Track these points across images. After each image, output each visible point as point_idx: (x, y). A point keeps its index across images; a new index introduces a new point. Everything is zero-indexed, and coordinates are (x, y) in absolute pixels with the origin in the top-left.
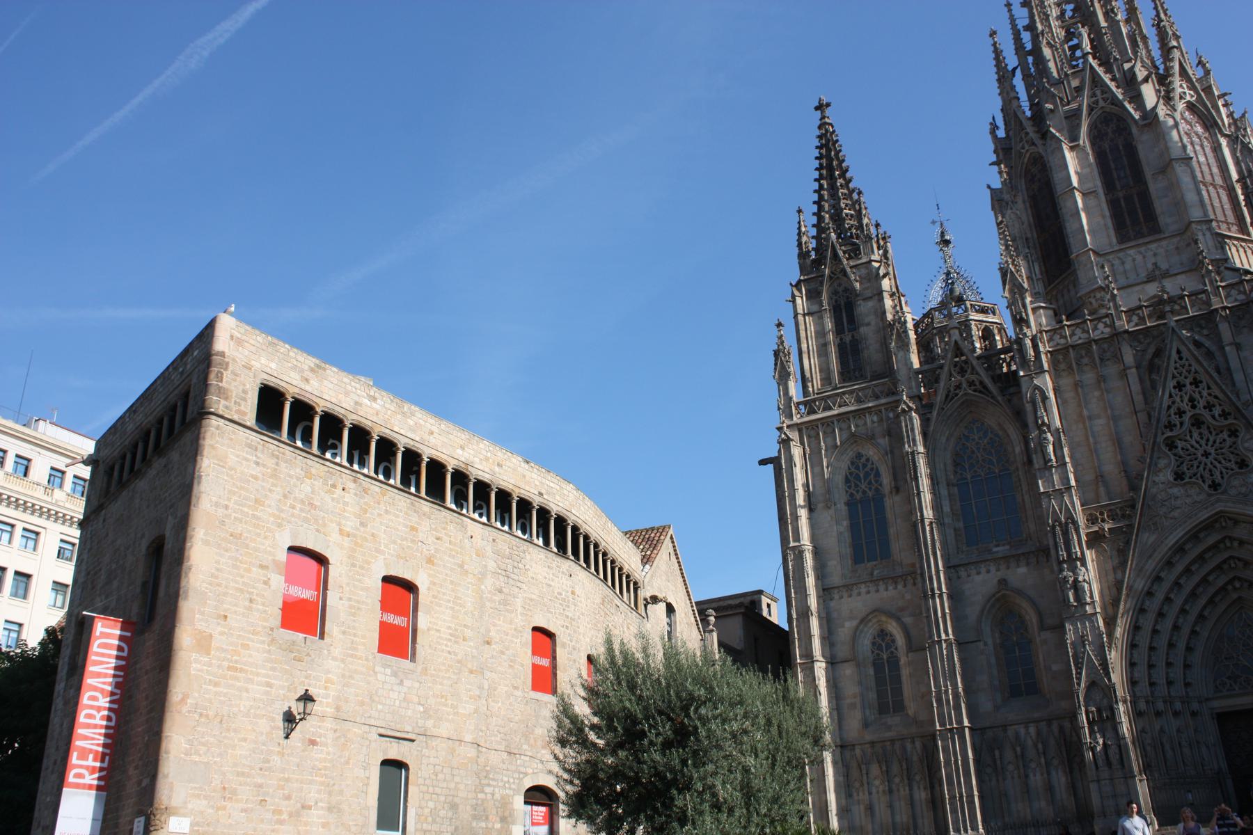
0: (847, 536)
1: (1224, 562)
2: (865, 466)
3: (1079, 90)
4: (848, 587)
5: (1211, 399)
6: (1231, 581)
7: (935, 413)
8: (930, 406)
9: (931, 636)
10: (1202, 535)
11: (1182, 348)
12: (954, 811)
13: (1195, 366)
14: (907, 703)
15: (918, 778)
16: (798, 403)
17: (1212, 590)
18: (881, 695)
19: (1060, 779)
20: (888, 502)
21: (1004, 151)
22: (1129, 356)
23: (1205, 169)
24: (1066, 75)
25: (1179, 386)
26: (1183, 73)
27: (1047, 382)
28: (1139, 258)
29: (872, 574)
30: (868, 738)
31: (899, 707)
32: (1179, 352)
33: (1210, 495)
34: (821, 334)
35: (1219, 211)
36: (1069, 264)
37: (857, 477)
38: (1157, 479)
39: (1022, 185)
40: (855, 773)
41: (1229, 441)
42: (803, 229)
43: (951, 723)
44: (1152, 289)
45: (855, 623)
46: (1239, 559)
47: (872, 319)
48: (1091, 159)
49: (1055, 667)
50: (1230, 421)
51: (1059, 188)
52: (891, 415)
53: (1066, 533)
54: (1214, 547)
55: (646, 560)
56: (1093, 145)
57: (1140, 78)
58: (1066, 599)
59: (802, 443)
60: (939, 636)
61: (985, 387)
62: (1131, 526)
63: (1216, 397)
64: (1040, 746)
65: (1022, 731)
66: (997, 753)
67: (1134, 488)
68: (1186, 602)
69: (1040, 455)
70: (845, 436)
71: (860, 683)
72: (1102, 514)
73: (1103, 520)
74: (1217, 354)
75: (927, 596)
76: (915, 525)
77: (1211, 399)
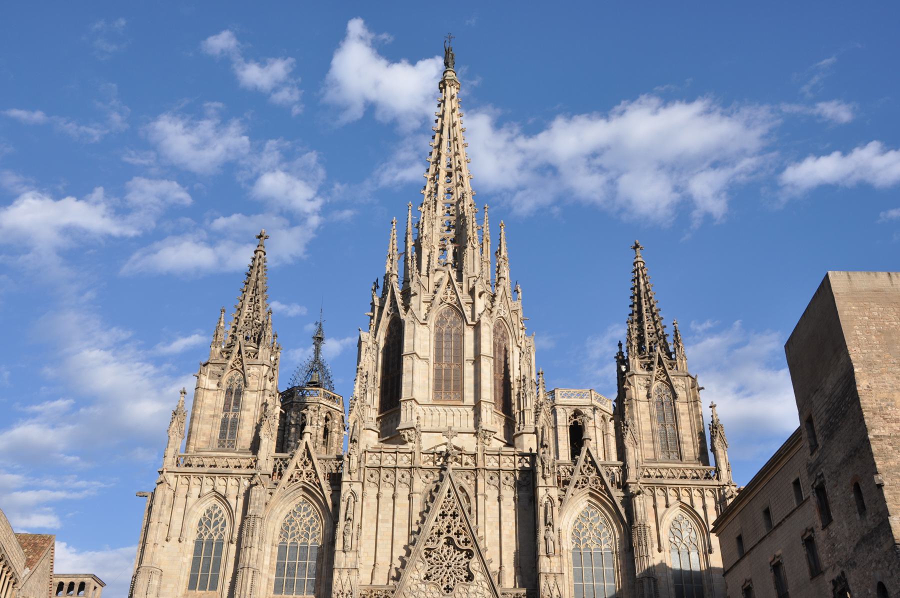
2: (216, 515)
7: (277, 491)
11: (452, 490)
13: (457, 504)
25: (443, 515)
28: (443, 414)
32: (449, 491)
37: (209, 523)
38: (412, 575)
44: (445, 440)
47: (252, 407)
48: (432, 336)
50: (469, 547)
51: (406, 350)
55: (29, 563)
56: (436, 326)
67: (397, 578)
72: (372, 592)
74: (473, 499)
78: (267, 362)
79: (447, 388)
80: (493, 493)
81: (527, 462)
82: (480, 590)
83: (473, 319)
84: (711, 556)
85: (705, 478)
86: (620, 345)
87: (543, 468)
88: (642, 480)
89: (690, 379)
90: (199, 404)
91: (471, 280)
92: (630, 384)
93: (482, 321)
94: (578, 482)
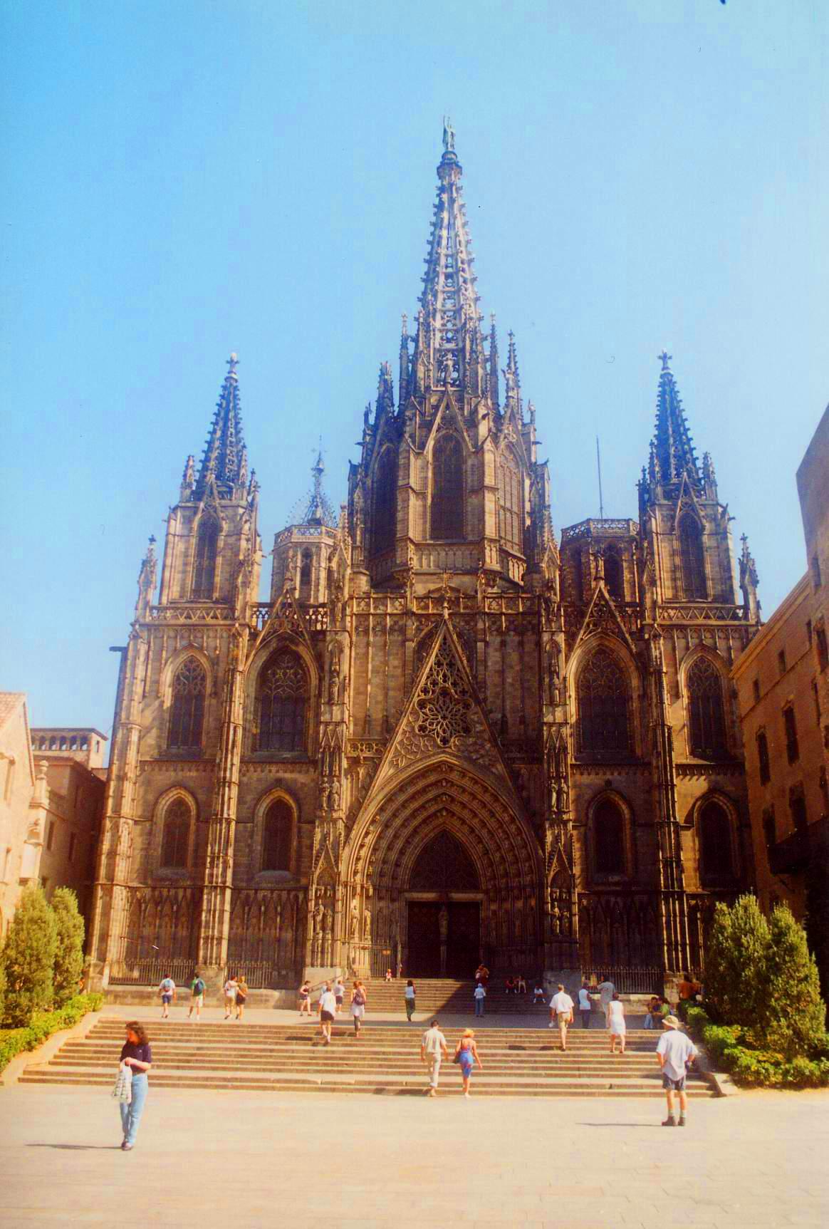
17: (425, 814)
25: (439, 664)
27: (345, 639)
32: (445, 639)
41: (462, 711)
53: (332, 755)
62: (380, 759)
86: (644, 470)
91: (474, 401)
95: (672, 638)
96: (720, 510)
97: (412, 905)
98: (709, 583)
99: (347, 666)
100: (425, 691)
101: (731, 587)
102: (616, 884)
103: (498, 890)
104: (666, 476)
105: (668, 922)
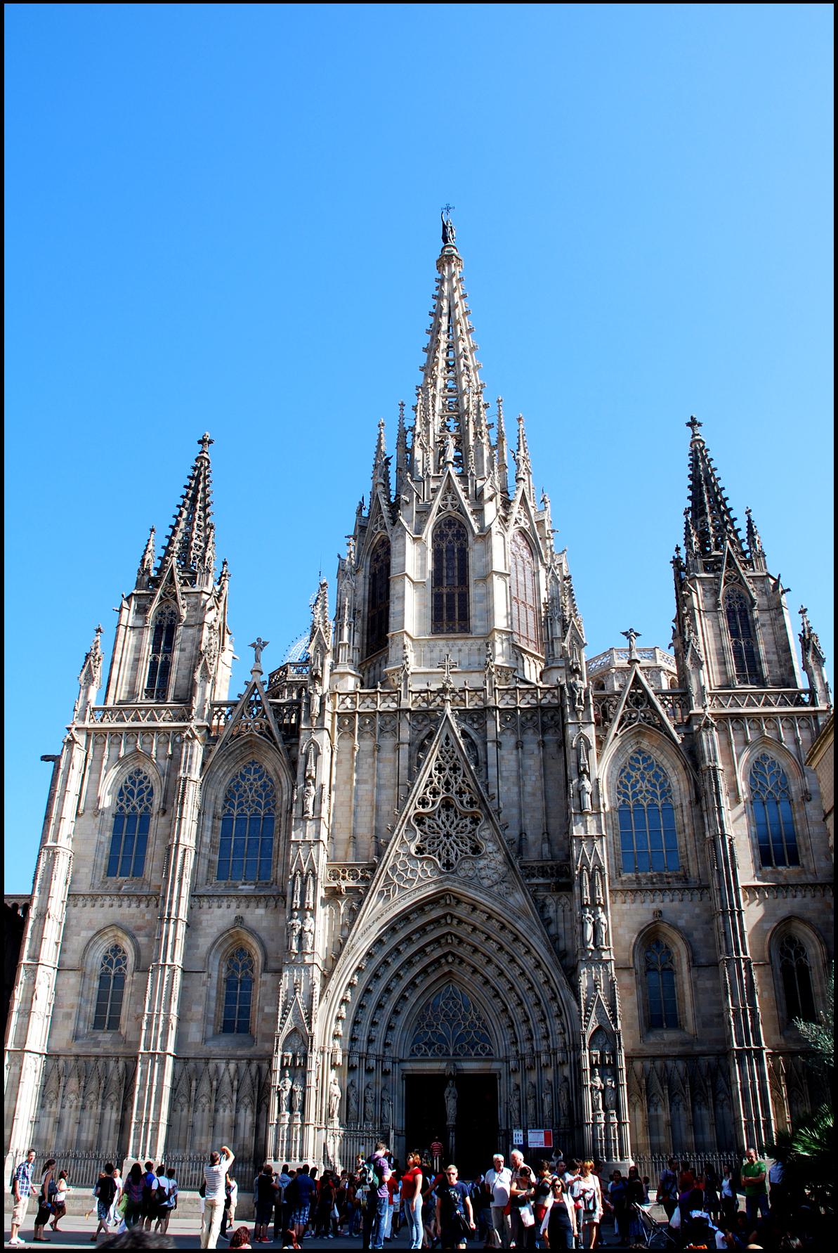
0: (106, 848)
1: (443, 936)
2: (141, 782)
3: (434, 491)
4: (94, 897)
5: (464, 787)
6: (445, 956)
7: (218, 746)
8: (216, 739)
9: (157, 960)
10: (427, 908)
11: (451, 736)
12: (137, 1136)
13: (457, 754)
14: (122, 1021)
15: (113, 1097)
16: (94, 709)
17: (427, 961)
18: (100, 1009)
19: (246, 1118)
20: (153, 822)
21: (362, 528)
22: (405, 734)
23: (521, 588)
24: (428, 476)
25: (440, 769)
26: (524, 501)
27: (323, 739)
28: (446, 651)
29: (120, 888)
30: (75, 1050)
31: (114, 1024)
32: (447, 738)
33: (442, 873)
34: (138, 649)
35: (523, 627)
36: (387, 640)
37: (131, 793)
39: (367, 561)
40: (53, 1084)
42: (150, 547)
43: (155, 1048)
45: (91, 933)
46: (456, 937)
49: (267, 1010)
50: (475, 809)
51: (394, 572)
52: (178, 739)
53: (304, 883)
54: (436, 921)
56: (433, 541)
57: (487, 495)
58: (289, 947)
59: (87, 748)
60: (165, 960)
61: (271, 733)
62: (367, 888)
63: (468, 785)
64: (236, 1083)
65: (223, 1066)
66: (194, 1084)
67: (380, 854)
68: (401, 967)
69: (300, 805)
70: (130, 750)
71: (81, 994)
72: (344, 871)
73: (344, 878)
74: (480, 747)
75: (162, 919)
76: (169, 849)
77: (464, 787)
78: (209, 590)
79: (451, 618)
80: (509, 740)
81: (554, 696)
82: (493, 865)
83: (481, 530)
84: (808, 806)
85: (796, 705)
86: (678, 549)
87: (572, 698)
88: (709, 710)
89: (772, 582)
90: (120, 645)
91: (479, 483)
92: (690, 591)
93: (494, 530)
94: (623, 718)
95: (727, 729)
96: (772, 582)
97: (412, 1081)
98: (765, 666)
99: (324, 771)
100: (423, 803)
101: (792, 668)
102: (672, 1043)
103: (520, 1058)
104: (704, 552)
105: (744, 1091)
